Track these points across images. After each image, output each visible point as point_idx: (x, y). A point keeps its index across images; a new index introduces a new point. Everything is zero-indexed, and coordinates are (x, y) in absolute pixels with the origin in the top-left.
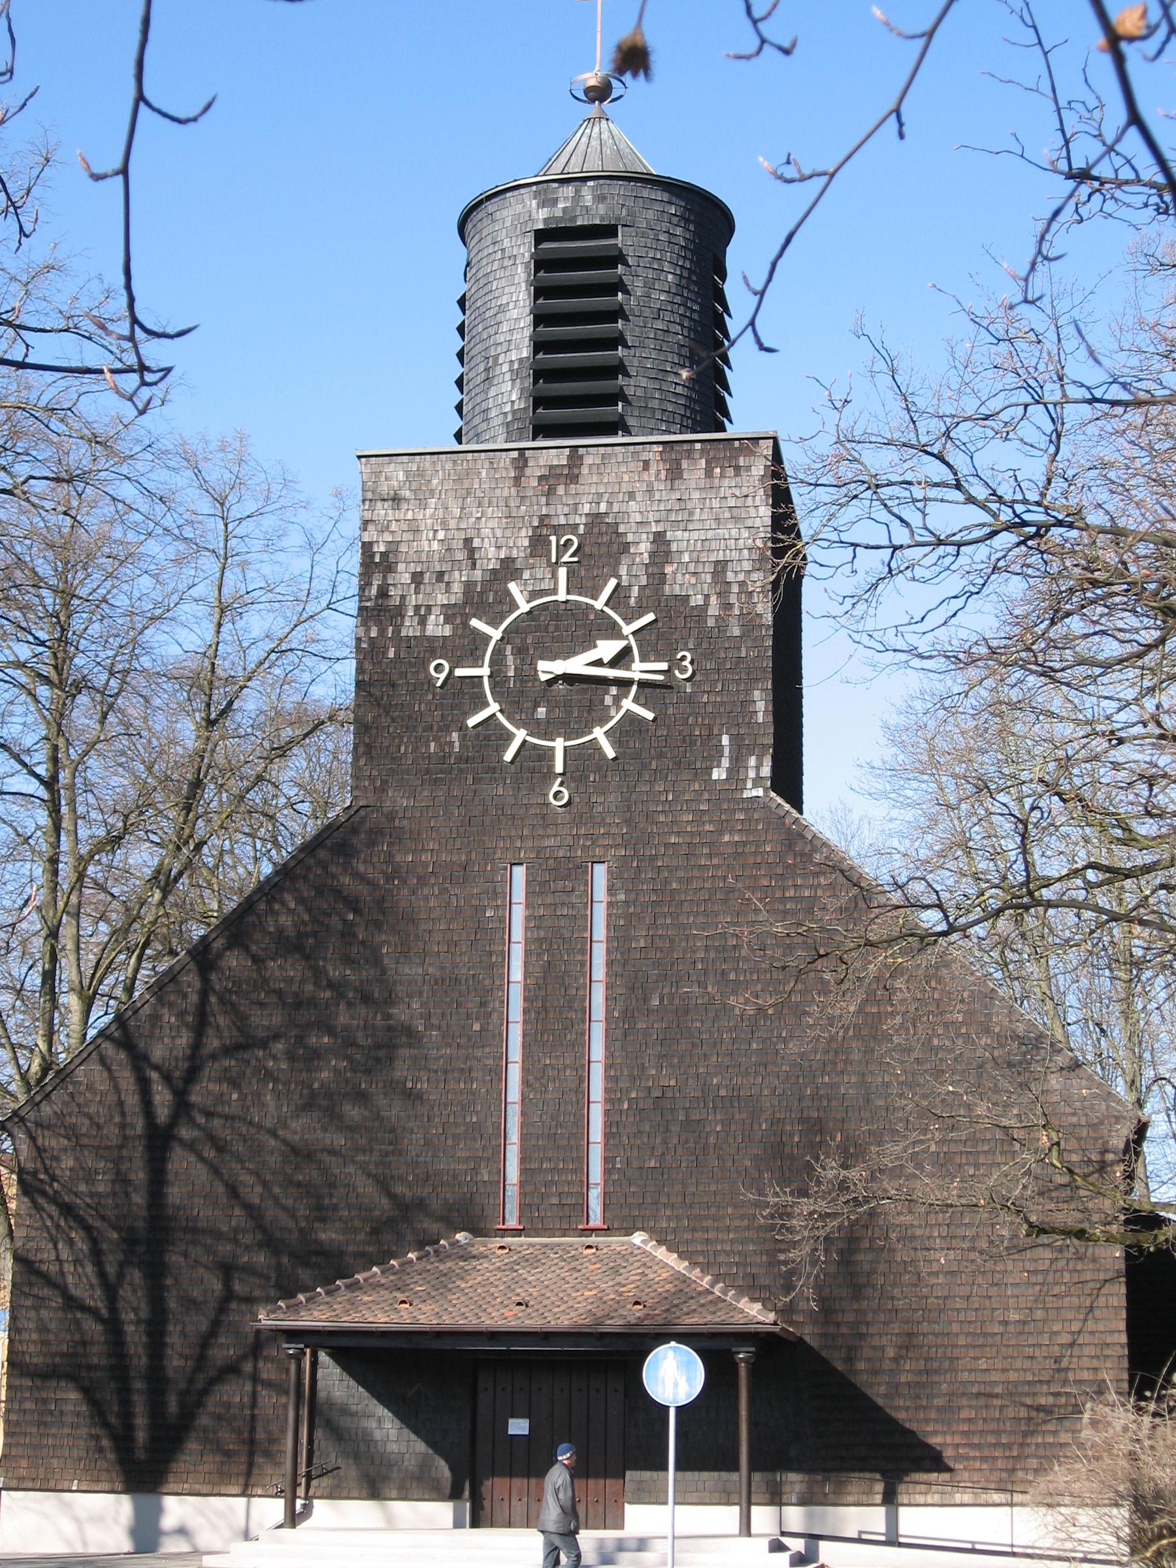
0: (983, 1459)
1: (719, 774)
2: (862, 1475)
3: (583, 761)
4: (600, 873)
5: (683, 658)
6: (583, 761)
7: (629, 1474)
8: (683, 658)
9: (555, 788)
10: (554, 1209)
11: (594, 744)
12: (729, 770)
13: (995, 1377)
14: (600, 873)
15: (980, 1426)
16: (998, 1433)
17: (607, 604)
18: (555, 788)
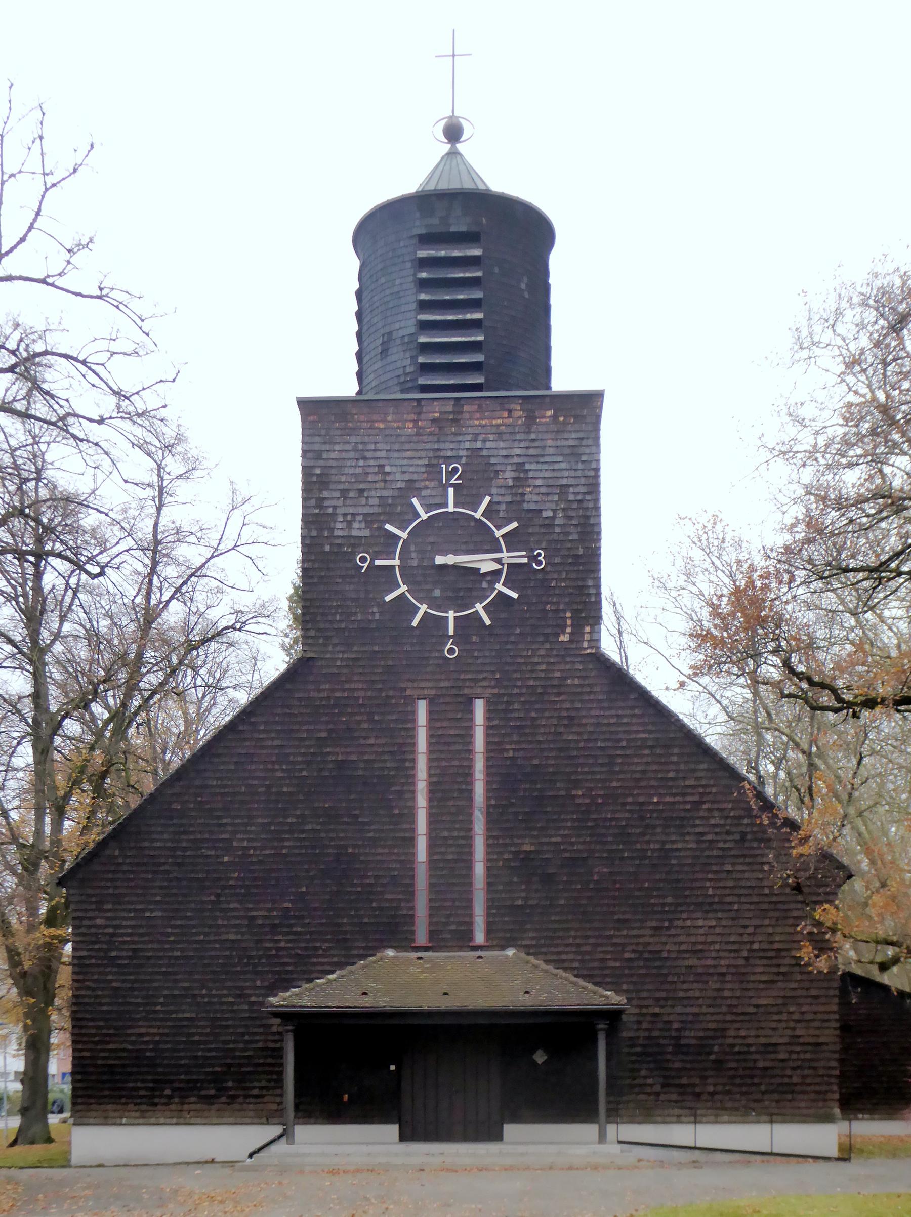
0: (743, 1093)
1: (565, 638)
2: (666, 1112)
3: (467, 624)
4: (479, 707)
5: (539, 554)
6: (467, 624)
7: (509, 1130)
8: (539, 554)
9: (449, 646)
10: (451, 935)
11: (476, 616)
12: (571, 634)
13: (750, 1041)
14: (479, 707)
15: (741, 1072)
16: (752, 1077)
17: (502, 536)
18: (449, 646)
